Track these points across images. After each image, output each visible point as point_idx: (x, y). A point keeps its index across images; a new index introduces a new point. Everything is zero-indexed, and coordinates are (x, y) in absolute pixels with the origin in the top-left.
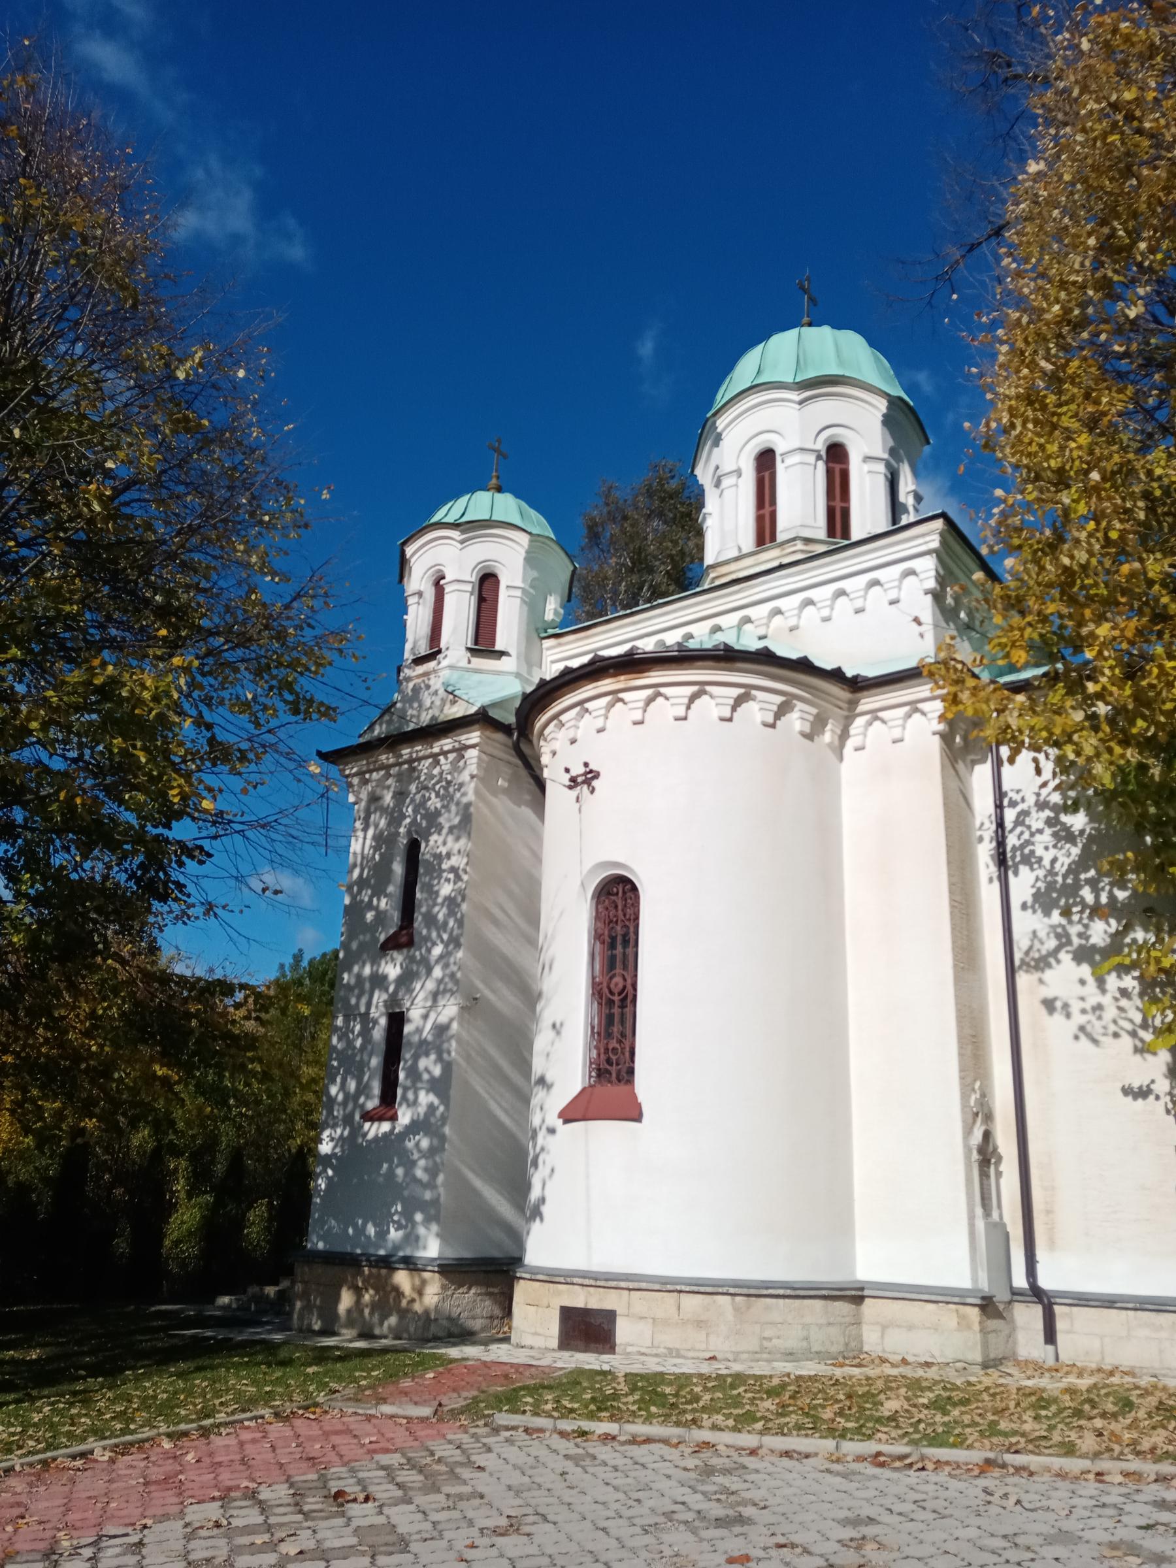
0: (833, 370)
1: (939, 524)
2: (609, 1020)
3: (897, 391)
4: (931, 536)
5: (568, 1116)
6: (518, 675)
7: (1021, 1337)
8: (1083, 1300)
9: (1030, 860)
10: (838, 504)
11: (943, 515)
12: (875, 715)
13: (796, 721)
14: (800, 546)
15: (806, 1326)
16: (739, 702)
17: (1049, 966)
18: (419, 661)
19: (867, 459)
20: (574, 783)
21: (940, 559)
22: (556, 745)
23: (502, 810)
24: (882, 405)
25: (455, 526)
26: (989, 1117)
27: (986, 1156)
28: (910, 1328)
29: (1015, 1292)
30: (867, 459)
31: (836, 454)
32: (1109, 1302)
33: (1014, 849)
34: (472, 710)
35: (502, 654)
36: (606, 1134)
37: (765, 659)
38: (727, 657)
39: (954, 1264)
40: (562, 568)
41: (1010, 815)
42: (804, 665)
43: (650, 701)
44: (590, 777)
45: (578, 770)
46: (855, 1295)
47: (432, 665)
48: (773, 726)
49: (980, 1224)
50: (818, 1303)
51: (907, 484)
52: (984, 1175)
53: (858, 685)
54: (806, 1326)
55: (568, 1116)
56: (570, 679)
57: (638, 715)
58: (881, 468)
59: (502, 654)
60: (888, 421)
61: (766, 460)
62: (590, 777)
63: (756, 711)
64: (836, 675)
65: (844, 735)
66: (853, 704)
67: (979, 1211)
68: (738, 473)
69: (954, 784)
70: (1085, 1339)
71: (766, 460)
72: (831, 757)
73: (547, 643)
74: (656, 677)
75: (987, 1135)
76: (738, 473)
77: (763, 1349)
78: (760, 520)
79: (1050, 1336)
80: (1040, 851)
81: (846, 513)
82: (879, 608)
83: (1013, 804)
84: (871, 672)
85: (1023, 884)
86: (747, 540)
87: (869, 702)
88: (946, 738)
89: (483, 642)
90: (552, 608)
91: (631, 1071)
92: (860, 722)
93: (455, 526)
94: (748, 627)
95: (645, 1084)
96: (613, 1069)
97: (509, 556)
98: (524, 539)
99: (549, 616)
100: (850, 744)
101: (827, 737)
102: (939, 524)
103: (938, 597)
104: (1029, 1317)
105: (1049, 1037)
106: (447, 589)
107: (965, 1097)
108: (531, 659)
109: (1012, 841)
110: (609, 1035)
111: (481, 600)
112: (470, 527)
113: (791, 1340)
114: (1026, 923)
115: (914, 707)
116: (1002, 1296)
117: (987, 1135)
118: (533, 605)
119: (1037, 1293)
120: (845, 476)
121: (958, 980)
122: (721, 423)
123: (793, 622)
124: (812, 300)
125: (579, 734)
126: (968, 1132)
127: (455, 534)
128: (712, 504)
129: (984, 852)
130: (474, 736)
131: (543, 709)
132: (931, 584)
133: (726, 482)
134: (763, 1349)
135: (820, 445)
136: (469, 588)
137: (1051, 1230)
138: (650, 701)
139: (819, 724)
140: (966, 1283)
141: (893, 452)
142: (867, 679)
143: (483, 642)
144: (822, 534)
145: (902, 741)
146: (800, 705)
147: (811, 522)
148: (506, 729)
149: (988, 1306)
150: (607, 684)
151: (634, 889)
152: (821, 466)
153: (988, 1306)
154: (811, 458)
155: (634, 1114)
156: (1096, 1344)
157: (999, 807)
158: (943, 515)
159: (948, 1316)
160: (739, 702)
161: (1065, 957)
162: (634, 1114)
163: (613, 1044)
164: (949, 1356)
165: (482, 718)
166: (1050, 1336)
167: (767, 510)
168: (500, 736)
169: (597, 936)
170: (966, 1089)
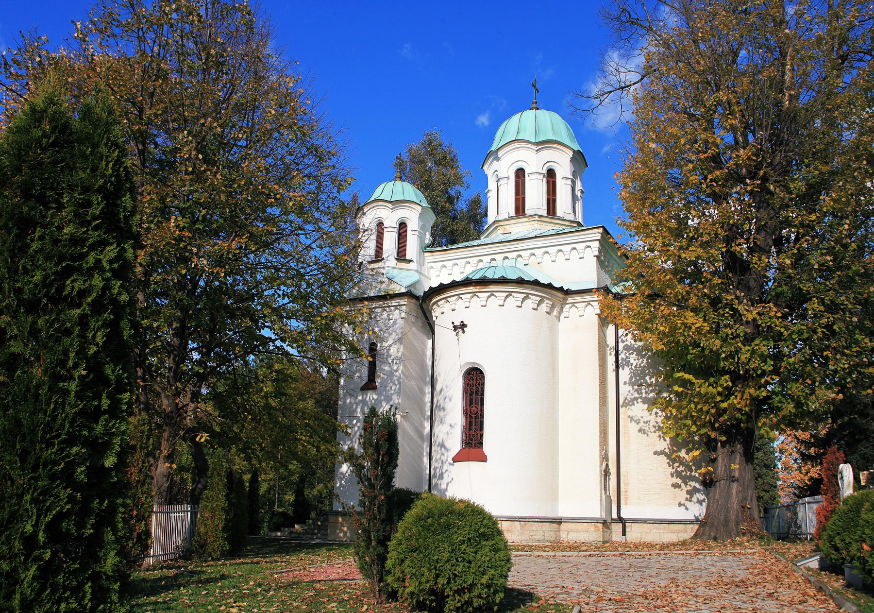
0: (551, 137)
1: (601, 230)
2: (471, 423)
3: (577, 147)
4: (597, 234)
5: (456, 459)
6: (417, 271)
7: (614, 534)
8: (636, 521)
9: (628, 364)
10: (551, 197)
11: (603, 227)
12: (573, 304)
13: (544, 307)
14: (537, 218)
15: (544, 532)
16: (524, 299)
17: (633, 404)
18: (370, 262)
19: (564, 178)
20: (455, 328)
21: (600, 243)
22: (443, 310)
23: (416, 334)
24: (571, 154)
25: (390, 202)
26: (607, 460)
27: (606, 473)
28: (578, 532)
29: (613, 519)
30: (564, 178)
31: (551, 174)
32: (644, 521)
33: (622, 359)
34: (403, 290)
35: (410, 261)
36: (474, 466)
37: (536, 283)
38: (520, 282)
39: (595, 511)
40: (432, 218)
41: (621, 345)
42: (550, 286)
43: (489, 297)
44: (463, 326)
45: (457, 323)
46: (559, 521)
47: (380, 264)
48: (536, 309)
49: (604, 496)
50: (548, 524)
51: (579, 186)
52: (605, 480)
53: (568, 293)
54: (544, 532)
55: (456, 459)
56: (454, 285)
57: (484, 303)
58: (569, 182)
59: (410, 261)
60: (572, 160)
61: (520, 174)
62: (463, 326)
63: (530, 303)
64: (561, 289)
65: (561, 311)
66: (565, 299)
67: (603, 492)
68: (508, 178)
69: (602, 334)
70: (635, 533)
71: (520, 174)
72: (556, 320)
73: (427, 254)
74: (492, 288)
75: (607, 465)
76: (508, 178)
77: (530, 539)
78: (517, 200)
79: (624, 533)
80: (632, 361)
81: (554, 201)
82: (576, 263)
83: (623, 341)
84: (573, 288)
85: (625, 374)
86: (513, 214)
87: (571, 299)
88: (599, 315)
89: (401, 256)
90: (428, 239)
91: (481, 444)
92: (568, 306)
93: (390, 202)
94: (519, 259)
95: (487, 448)
96: (473, 442)
97: (413, 217)
98: (419, 208)
99: (427, 241)
100: (563, 315)
101: (555, 313)
102: (601, 230)
103: (598, 257)
104: (617, 528)
105: (629, 430)
106: (385, 230)
107: (601, 452)
108: (421, 263)
109: (622, 356)
110: (470, 430)
111: (400, 235)
112: (397, 203)
113: (539, 536)
114: (625, 389)
115: (589, 303)
116: (609, 521)
117: (607, 465)
118: (421, 238)
119: (620, 520)
120: (554, 183)
121: (600, 410)
122: (500, 154)
123: (540, 260)
124: (537, 90)
125: (456, 307)
126: (601, 465)
127: (390, 205)
128: (492, 185)
129: (611, 360)
130: (404, 301)
131: (439, 294)
132: (597, 253)
133: (501, 182)
134: (530, 539)
135: (545, 172)
136: (395, 230)
137: (626, 498)
138: (489, 297)
139: (553, 307)
140: (598, 516)
141: (574, 174)
142: (571, 291)
143: (401, 256)
144: (545, 213)
145: (583, 316)
146: (546, 301)
147: (540, 207)
148: (417, 298)
149: (604, 523)
150: (471, 289)
151: (481, 372)
152: (545, 180)
153: (604, 523)
154: (541, 177)
155: (483, 459)
156: (639, 535)
157: (617, 342)
158: (603, 227)
159: (591, 527)
160: (524, 299)
161: (640, 400)
162: (483, 459)
163: (472, 433)
164: (591, 539)
165: (409, 294)
166: (624, 533)
167: (521, 197)
168: (414, 301)
169: (465, 391)
170: (601, 449)
